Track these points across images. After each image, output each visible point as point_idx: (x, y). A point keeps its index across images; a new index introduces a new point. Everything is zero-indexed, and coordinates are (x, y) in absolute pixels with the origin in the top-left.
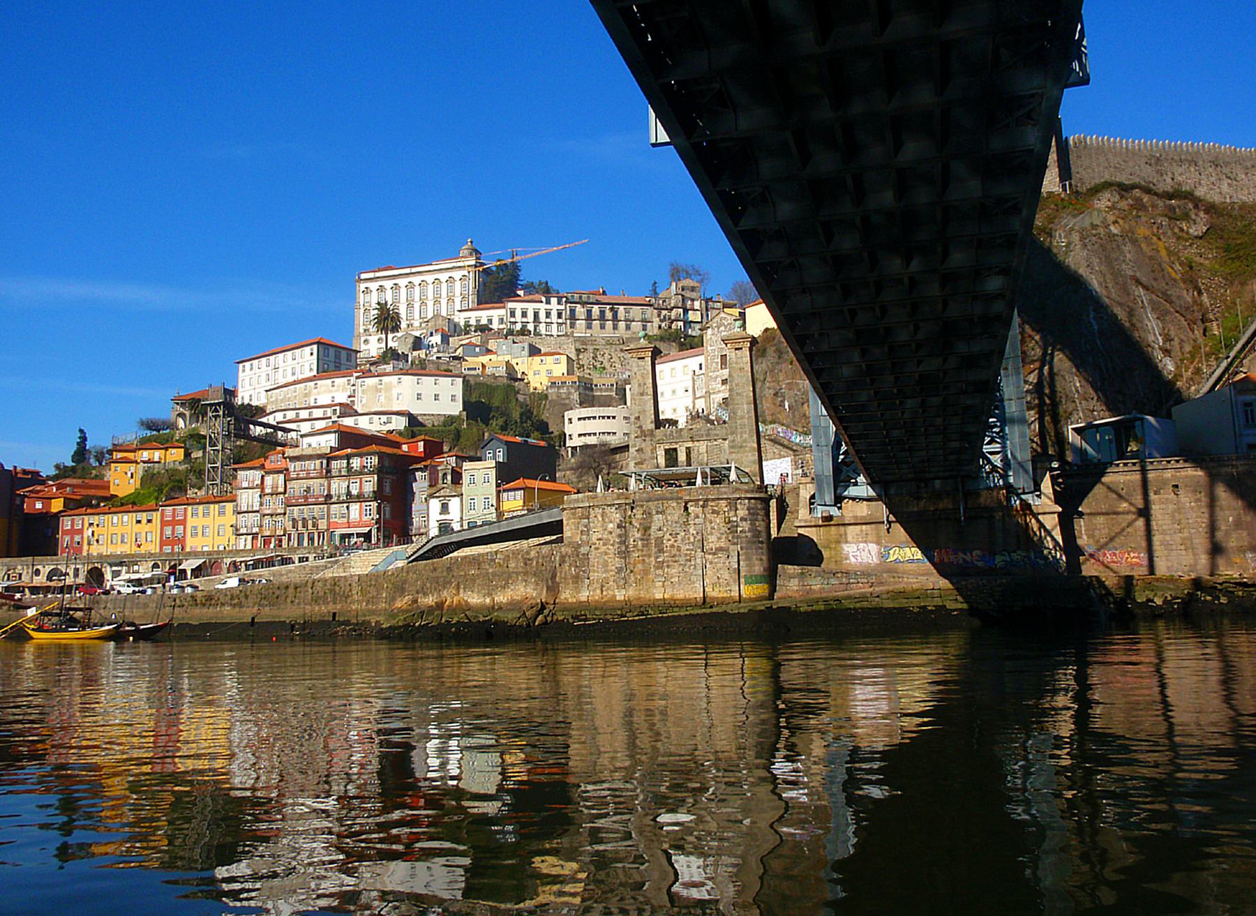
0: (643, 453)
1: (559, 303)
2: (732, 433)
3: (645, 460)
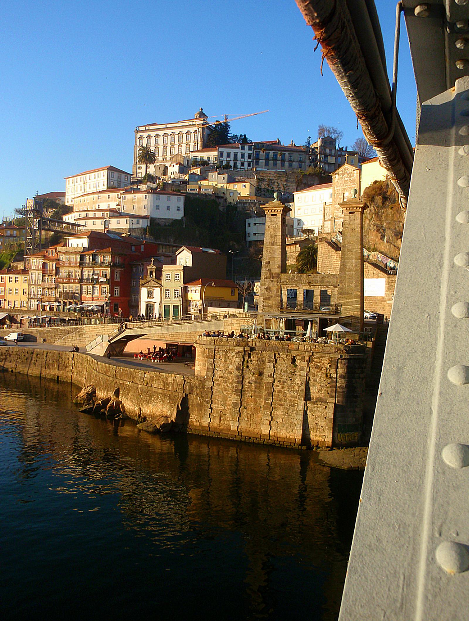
0: (270, 291)
1: (250, 149)
2: (341, 282)
3: (272, 297)
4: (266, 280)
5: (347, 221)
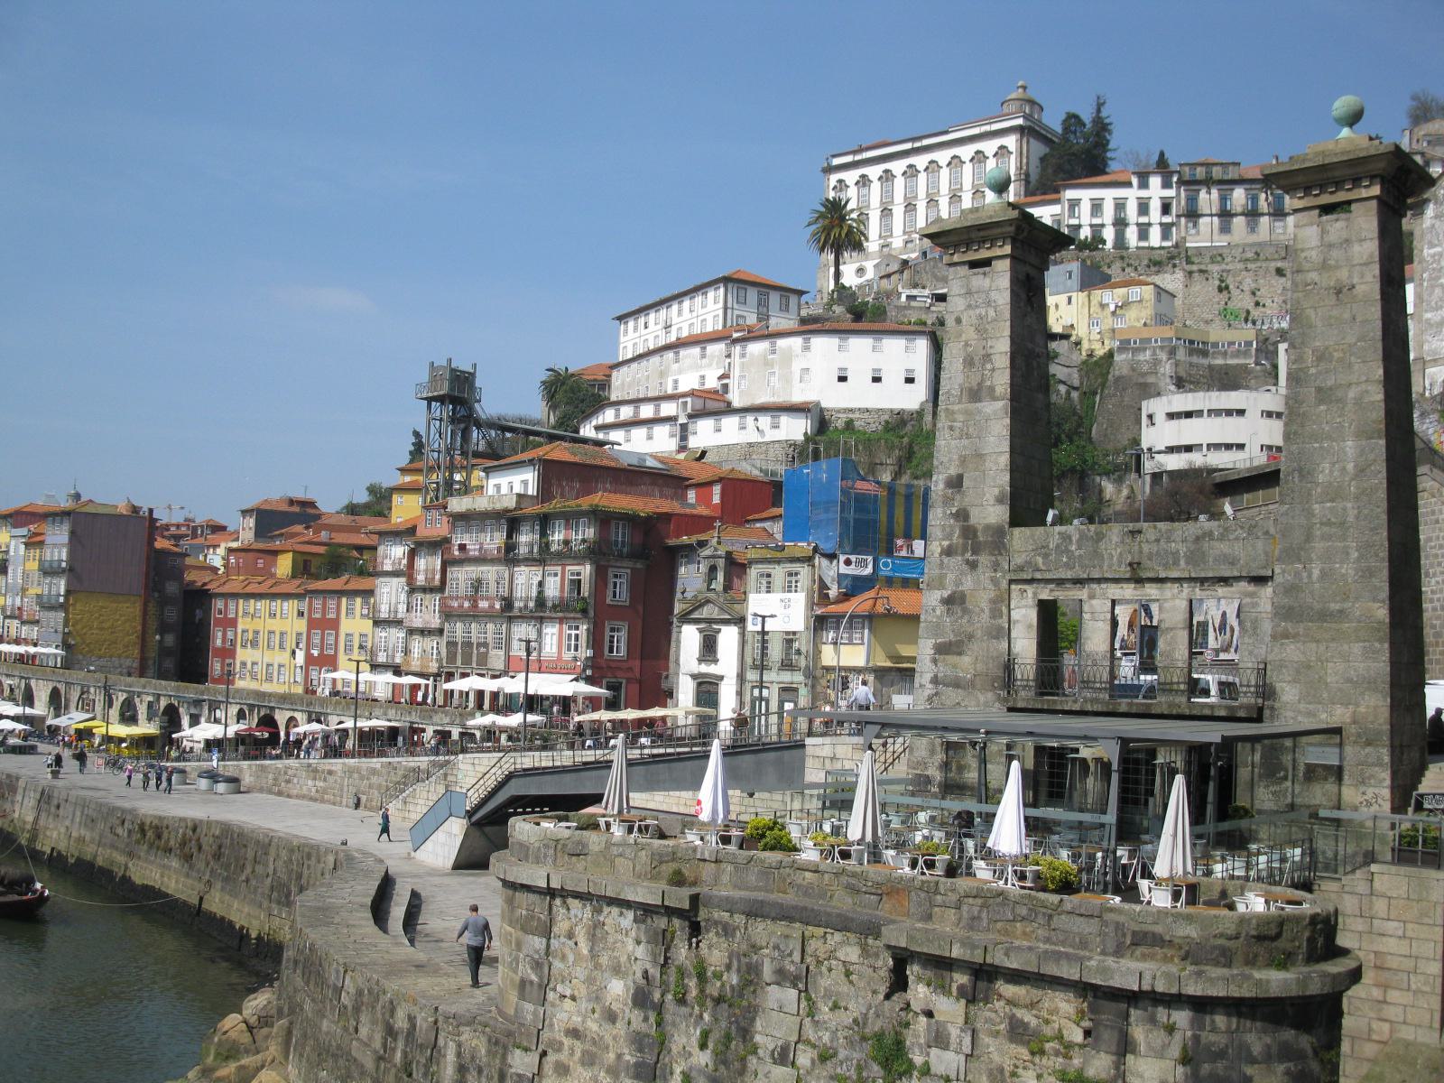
0: (965, 611)
1: (1166, 185)
2: (1293, 554)
3: (971, 637)
4: (946, 560)
5: (1314, 253)
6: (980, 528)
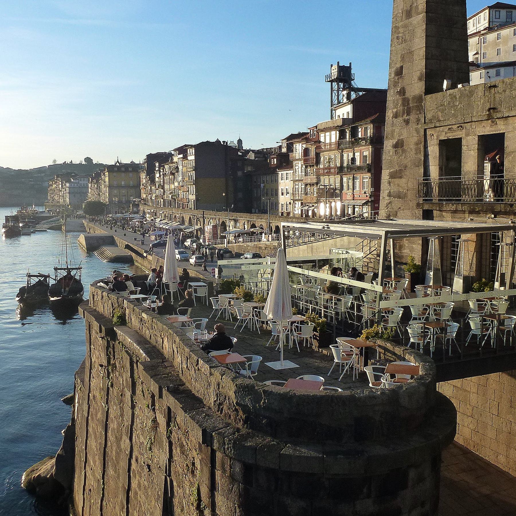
6: (410, 98)
